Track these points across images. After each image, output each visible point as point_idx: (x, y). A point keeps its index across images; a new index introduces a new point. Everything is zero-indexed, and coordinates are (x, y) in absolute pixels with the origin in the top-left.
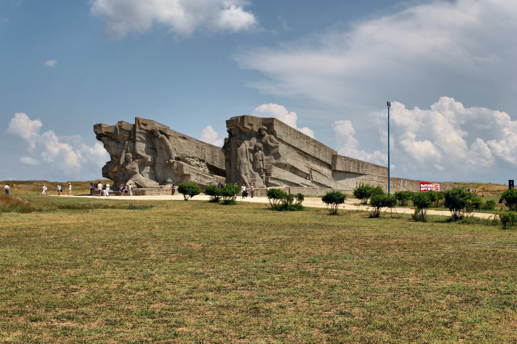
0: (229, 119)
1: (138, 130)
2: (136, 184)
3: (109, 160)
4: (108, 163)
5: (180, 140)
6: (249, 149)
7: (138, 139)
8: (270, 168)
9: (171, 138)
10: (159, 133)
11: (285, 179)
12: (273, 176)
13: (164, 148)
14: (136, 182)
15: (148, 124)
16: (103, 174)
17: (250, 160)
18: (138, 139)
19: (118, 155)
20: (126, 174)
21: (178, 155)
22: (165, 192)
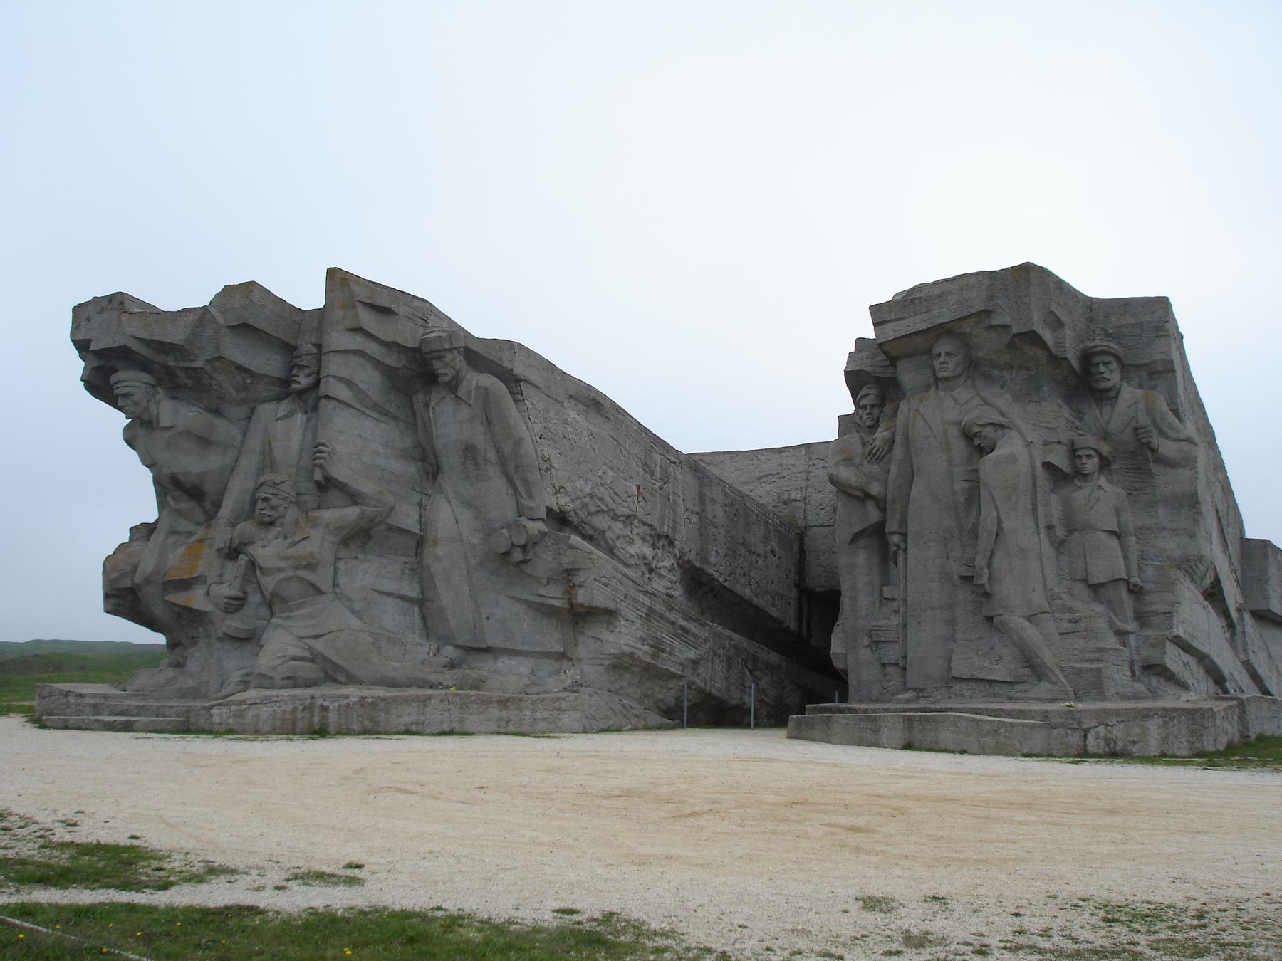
0: (886, 296)
1: (338, 339)
2: (314, 657)
3: (149, 512)
4: (142, 532)
5: (573, 414)
6: (1047, 465)
7: (342, 392)
8: (1167, 586)
9: (533, 399)
10: (459, 361)
11: (1205, 649)
12: (1180, 631)
13: (492, 455)
14: (318, 645)
15: (401, 309)
16: (107, 596)
17: (1050, 528)
18: (342, 392)
19: (209, 487)
20: (254, 599)
21: (564, 500)
22: (494, 712)
